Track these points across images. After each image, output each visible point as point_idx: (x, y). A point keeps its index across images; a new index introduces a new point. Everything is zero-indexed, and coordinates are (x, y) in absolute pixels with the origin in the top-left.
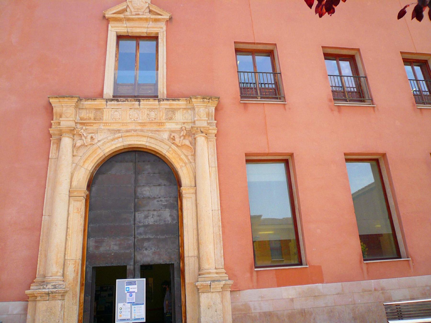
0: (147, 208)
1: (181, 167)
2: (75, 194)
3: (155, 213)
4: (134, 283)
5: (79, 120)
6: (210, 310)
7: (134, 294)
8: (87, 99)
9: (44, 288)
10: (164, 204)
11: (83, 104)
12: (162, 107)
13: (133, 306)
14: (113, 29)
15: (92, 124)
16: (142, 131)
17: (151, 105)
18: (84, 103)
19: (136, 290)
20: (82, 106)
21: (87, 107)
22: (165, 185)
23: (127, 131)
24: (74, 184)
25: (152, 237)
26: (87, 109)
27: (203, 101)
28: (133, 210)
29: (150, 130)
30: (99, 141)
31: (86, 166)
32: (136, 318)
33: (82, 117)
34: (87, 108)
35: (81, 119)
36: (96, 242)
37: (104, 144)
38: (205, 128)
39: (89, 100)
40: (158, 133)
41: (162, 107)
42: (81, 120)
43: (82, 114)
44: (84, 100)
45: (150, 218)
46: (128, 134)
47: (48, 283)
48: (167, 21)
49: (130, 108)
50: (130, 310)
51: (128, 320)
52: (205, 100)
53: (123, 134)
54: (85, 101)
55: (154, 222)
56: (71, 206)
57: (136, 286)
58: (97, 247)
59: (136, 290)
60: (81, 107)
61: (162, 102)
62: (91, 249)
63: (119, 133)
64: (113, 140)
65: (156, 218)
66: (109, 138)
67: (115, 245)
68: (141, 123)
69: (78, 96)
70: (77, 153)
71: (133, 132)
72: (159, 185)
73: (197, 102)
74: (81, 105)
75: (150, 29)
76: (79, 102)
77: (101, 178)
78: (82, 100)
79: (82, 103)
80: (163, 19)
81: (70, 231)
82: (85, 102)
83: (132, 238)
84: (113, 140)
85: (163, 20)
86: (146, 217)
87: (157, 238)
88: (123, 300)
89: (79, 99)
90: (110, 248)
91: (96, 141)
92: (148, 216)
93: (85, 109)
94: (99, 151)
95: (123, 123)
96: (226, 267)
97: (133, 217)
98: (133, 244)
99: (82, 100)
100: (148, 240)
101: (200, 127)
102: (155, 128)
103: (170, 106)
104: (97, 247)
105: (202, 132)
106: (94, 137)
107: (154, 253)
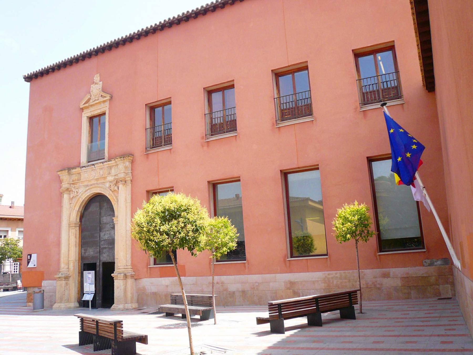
0: (104, 230)
1: (115, 204)
2: (71, 225)
3: (108, 232)
4: (89, 273)
6: (118, 289)
7: (90, 279)
9: (59, 275)
10: (112, 226)
12: (105, 166)
13: (90, 285)
14: (85, 115)
15: (76, 184)
16: (97, 184)
17: (100, 166)
19: (91, 277)
22: (112, 215)
23: (91, 185)
24: (71, 220)
25: (107, 247)
27: (121, 160)
28: (99, 230)
29: (101, 183)
30: (80, 193)
31: (76, 208)
32: (91, 291)
35: (73, 181)
36: (85, 250)
37: (82, 195)
38: (122, 179)
40: (104, 184)
41: (105, 166)
45: (106, 235)
46: (91, 187)
47: (60, 272)
48: (110, 100)
49: (92, 170)
50: (89, 287)
51: (88, 292)
52: (122, 159)
53: (89, 187)
55: (108, 237)
56: (70, 232)
57: (91, 275)
58: (85, 253)
59: (91, 277)
61: (104, 164)
62: (83, 254)
63: (88, 186)
64: (86, 191)
65: (108, 235)
66: (84, 191)
67: (92, 251)
68: (96, 179)
70: (72, 201)
71: (93, 185)
72: (110, 215)
73: (118, 161)
75: (102, 109)
77: (86, 213)
80: (107, 100)
81: (70, 246)
83: (99, 247)
84: (86, 191)
85: (107, 100)
86: (105, 235)
87: (109, 247)
88: (86, 282)
90: (90, 253)
91: (79, 193)
92: (105, 235)
94: (81, 199)
95: (89, 180)
96: (133, 264)
97: (99, 235)
98: (99, 251)
100: (105, 248)
101: (119, 178)
102: (102, 181)
103: (109, 165)
104: (85, 253)
105: (121, 181)
106: (78, 191)
107: (108, 256)
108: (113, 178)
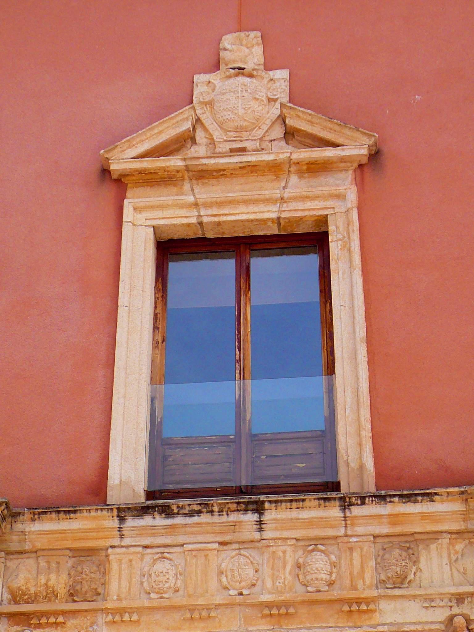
5: (5, 602)
8: (42, 510)
11: (23, 532)
12: (360, 530)
14: (141, 218)
15: (60, 619)
17: (310, 523)
18: (27, 530)
20: (20, 541)
21: (39, 545)
26: (39, 553)
33: (19, 589)
34: (40, 550)
39: (48, 516)
41: (360, 530)
42: (15, 600)
43: (17, 576)
44: (28, 516)
48: (361, 166)
54: (33, 520)
60: (14, 546)
61: (356, 511)
68: (269, 605)
69: (3, 500)
74: (15, 538)
75: (293, 205)
76: (9, 526)
78: (21, 517)
79: (19, 527)
80: (343, 160)
82: (32, 525)
85: (342, 165)
89: (6, 511)
93: (31, 552)
95: (192, 609)
99: (19, 514)
103: (393, 524)
108: (441, 615)
